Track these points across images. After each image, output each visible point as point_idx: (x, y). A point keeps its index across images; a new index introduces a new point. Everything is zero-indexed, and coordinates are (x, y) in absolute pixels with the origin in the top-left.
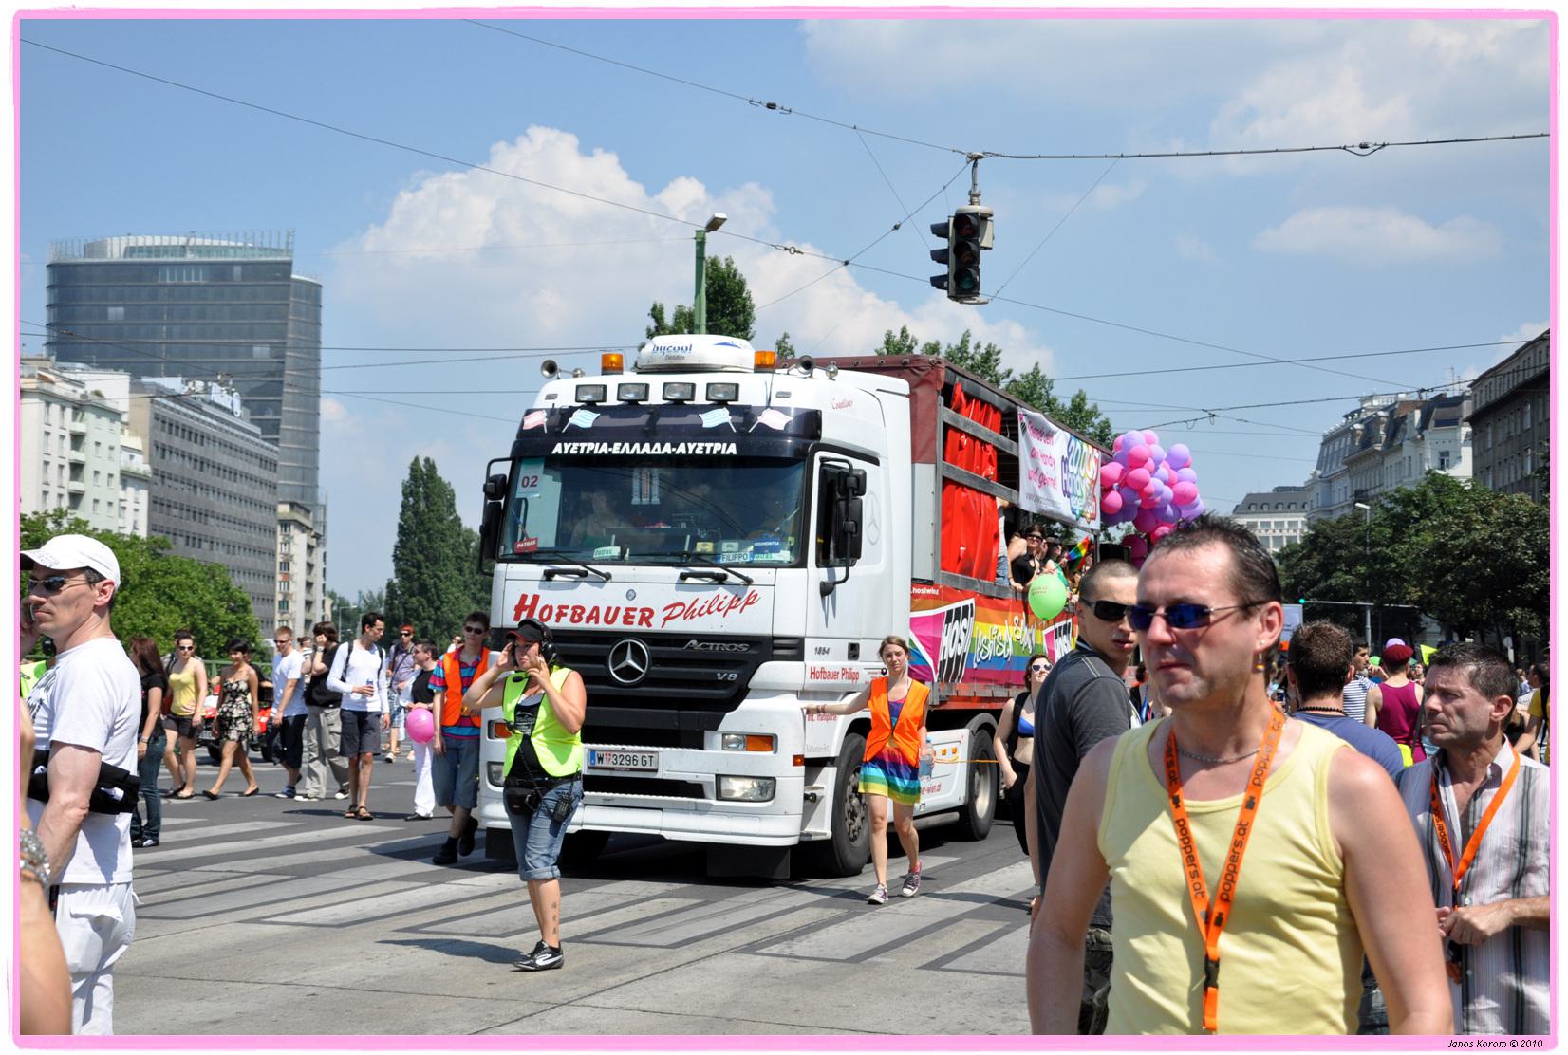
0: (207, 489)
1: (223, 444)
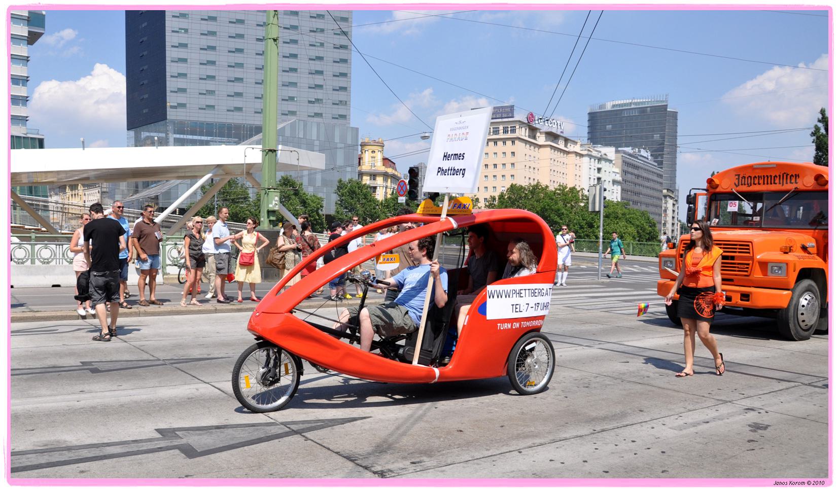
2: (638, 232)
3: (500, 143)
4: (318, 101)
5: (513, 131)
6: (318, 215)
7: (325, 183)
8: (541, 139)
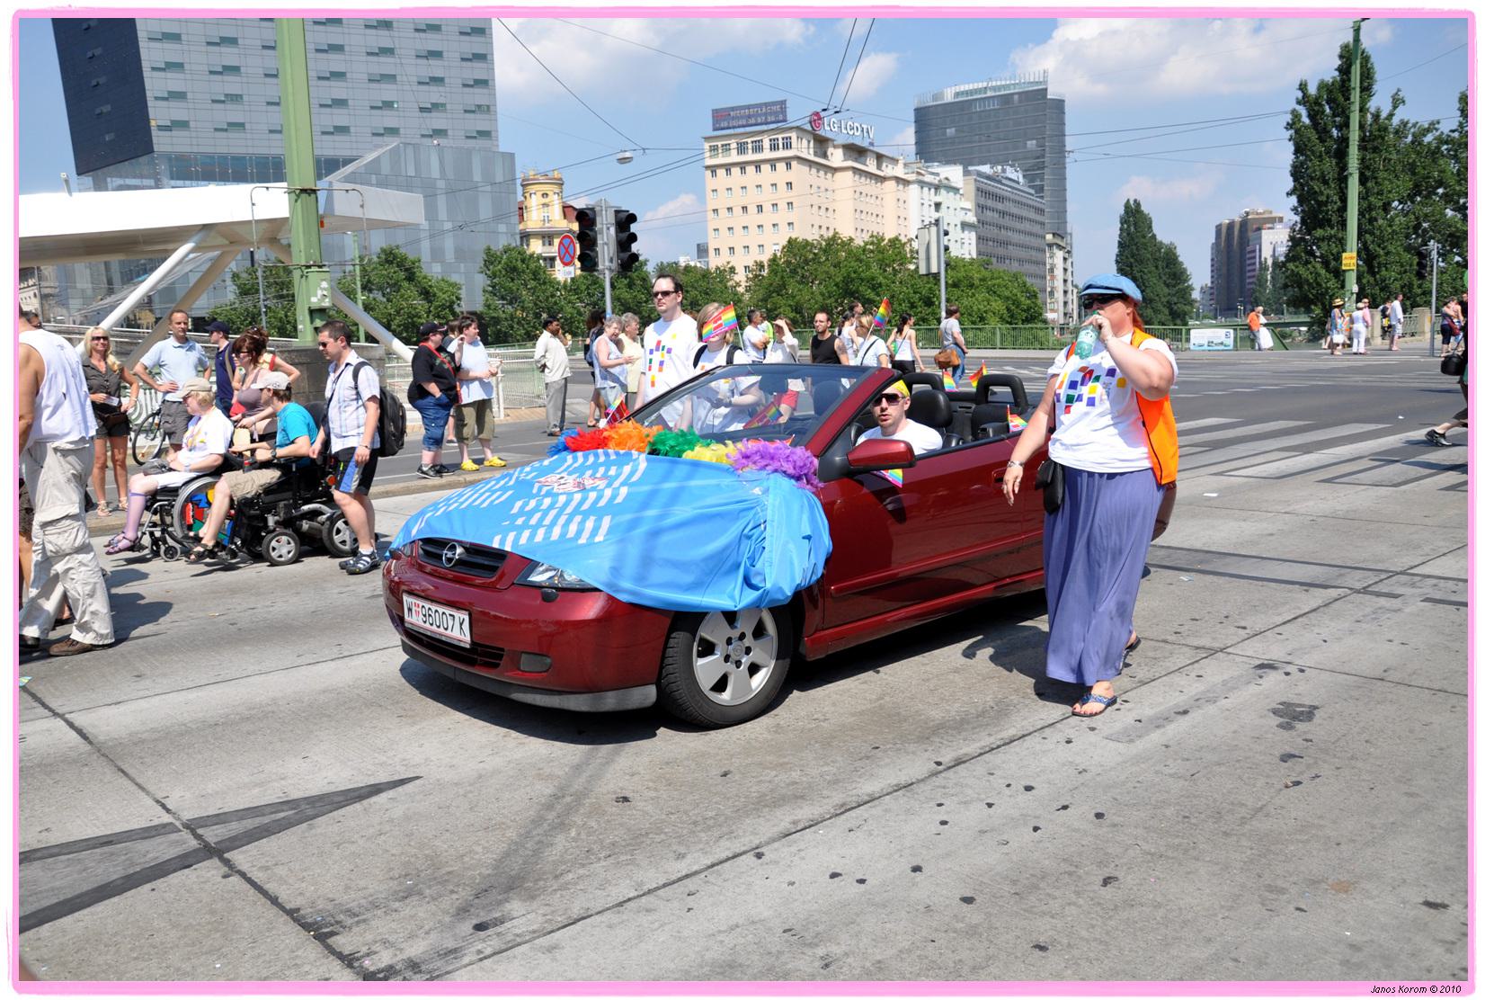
1: (1015, 201)
2: (1008, 309)
3: (766, 168)
4: (436, 107)
5: (788, 146)
6: (454, 313)
7: (460, 254)
8: (836, 157)
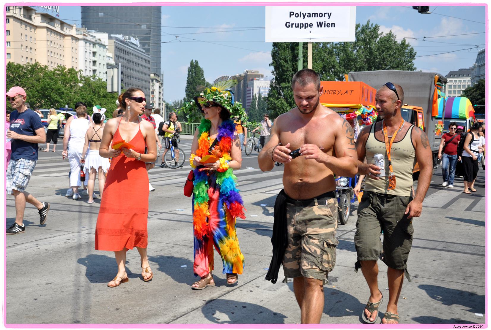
0: (131, 69)
